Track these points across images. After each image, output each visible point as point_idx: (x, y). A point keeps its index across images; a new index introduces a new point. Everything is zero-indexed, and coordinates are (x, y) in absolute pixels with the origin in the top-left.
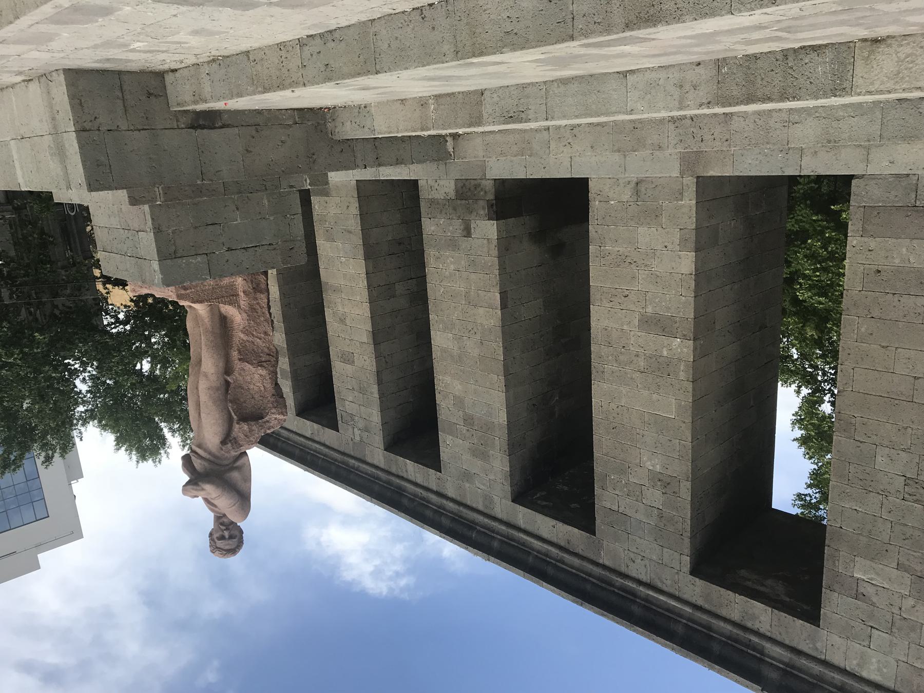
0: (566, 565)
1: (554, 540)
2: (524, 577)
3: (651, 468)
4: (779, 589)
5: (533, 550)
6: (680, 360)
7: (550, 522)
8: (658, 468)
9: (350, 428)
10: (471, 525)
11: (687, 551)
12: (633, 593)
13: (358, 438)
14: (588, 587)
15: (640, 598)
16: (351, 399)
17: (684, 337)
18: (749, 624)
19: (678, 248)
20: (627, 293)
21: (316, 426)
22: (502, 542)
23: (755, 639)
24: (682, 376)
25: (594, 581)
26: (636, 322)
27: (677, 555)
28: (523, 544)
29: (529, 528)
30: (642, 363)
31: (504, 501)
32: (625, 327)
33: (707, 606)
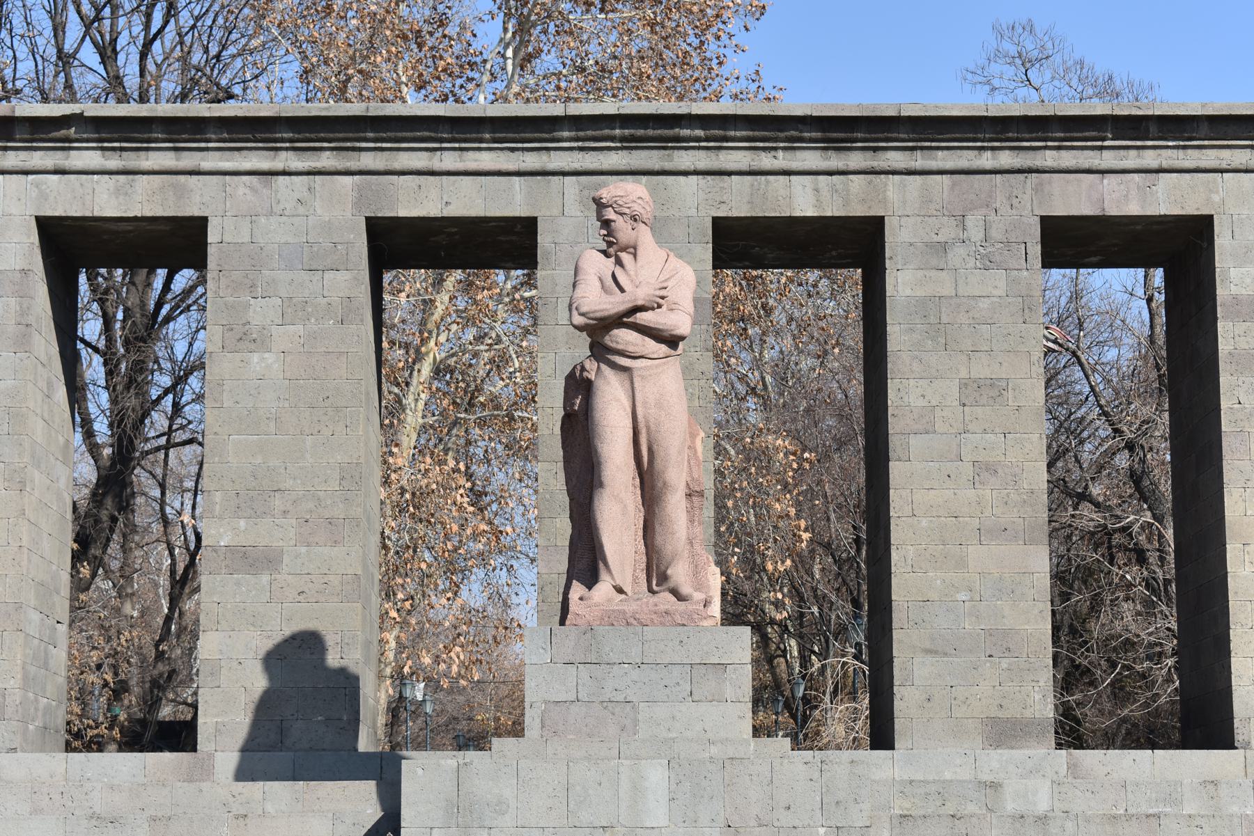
3: (266, 355)
4: (113, 226)
6: (221, 518)
8: (255, 357)
9: (995, 234)
10: (630, 143)
11: (211, 250)
13: (974, 221)
16: (984, 304)
17: (215, 549)
18: (122, 178)
19: (223, 663)
20: (301, 598)
21: (1133, 209)
23: (114, 162)
24: (218, 497)
25: (364, 145)
26: (286, 559)
27: (227, 238)
30: (278, 502)
31: (556, 212)
32: (303, 550)
33: (182, 178)
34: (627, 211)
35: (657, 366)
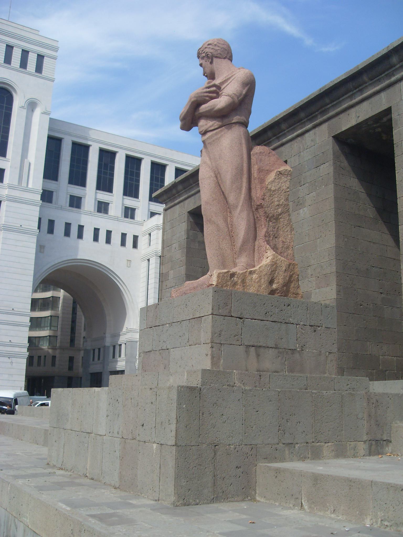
0: (347, 98)
1: (357, 108)
2: (358, 67)
3: (305, 209)
5: (370, 84)
7: (361, 119)
8: (301, 211)
12: (311, 120)
14: (327, 100)
15: (307, 121)
22: (392, 67)
25: (329, 106)
26: (313, 296)
28: (379, 80)
29: (377, 98)
32: (317, 290)
34: (204, 55)
35: (216, 134)
